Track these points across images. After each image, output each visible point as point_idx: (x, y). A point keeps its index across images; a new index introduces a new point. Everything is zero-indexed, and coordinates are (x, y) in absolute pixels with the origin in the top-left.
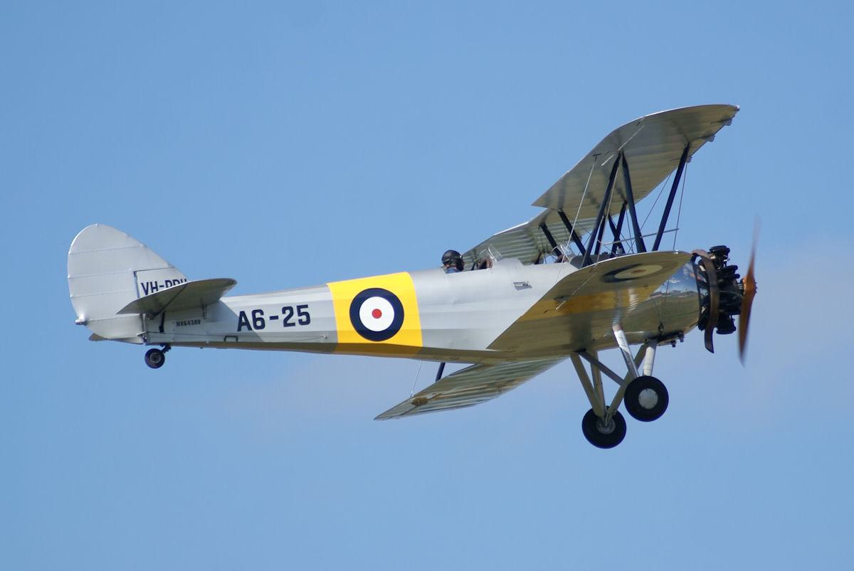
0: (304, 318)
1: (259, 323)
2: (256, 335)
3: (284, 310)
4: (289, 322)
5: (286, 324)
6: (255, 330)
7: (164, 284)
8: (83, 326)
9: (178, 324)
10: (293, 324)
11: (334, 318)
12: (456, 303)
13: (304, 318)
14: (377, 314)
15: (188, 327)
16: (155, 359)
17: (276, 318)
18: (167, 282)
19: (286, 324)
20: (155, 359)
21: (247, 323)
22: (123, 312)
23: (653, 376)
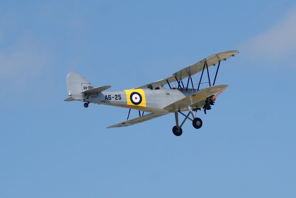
0: (120, 98)
1: (110, 98)
2: (109, 101)
3: (115, 95)
4: (116, 99)
5: (116, 99)
9: (92, 97)
10: (117, 99)
11: (126, 99)
12: (153, 97)
13: (120, 98)
14: (136, 98)
16: (86, 105)
17: (114, 97)
18: (89, 87)
19: (116, 99)
20: (86, 105)
21: (107, 98)
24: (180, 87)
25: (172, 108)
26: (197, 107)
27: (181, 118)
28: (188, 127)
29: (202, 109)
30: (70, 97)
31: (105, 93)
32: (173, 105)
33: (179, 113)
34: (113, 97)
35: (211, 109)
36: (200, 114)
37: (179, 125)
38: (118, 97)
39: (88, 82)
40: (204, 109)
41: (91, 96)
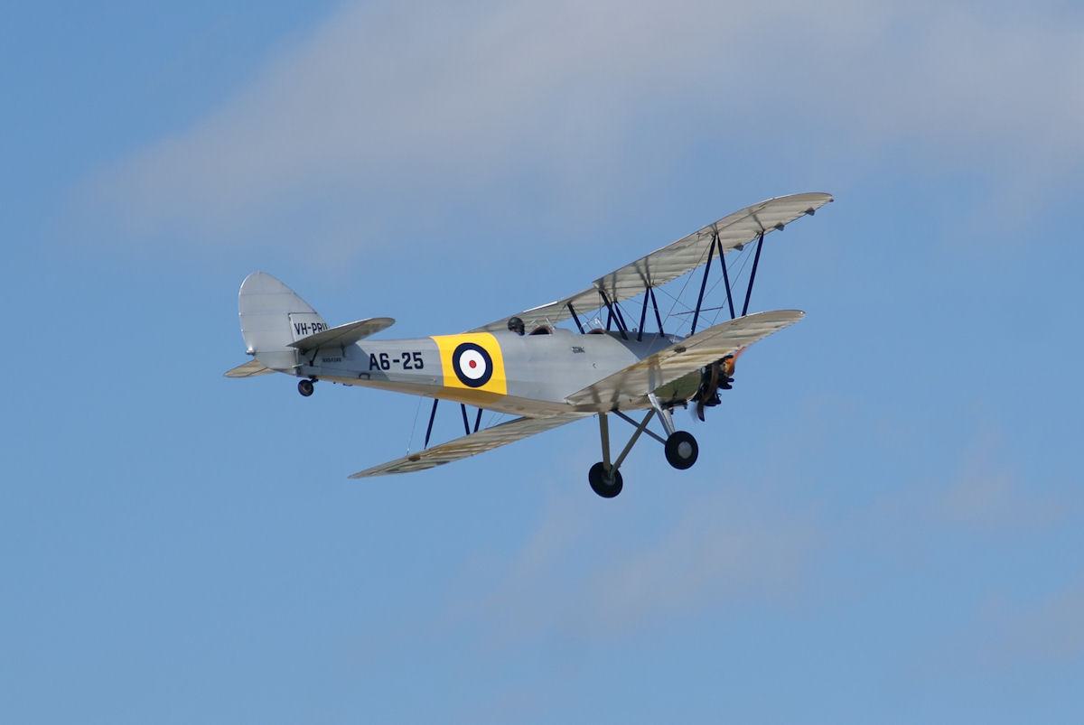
0: (418, 363)
1: (385, 365)
2: (384, 375)
3: (404, 355)
4: (407, 365)
5: (405, 368)
7: (310, 326)
8: (251, 356)
9: (324, 360)
10: (411, 368)
13: (418, 363)
14: (473, 364)
15: (332, 363)
16: (307, 388)
17: (398, 361)
19: (405, 368)
20: (306, 388)
21: (376, 364)
22: (289, 346)
23: (676, 431)
24: (614, 328)
25: (589, 401)
26: (675, 394)
27: (620, 432)
28: (645, 465)
29: (691, 404)
30: (251, 357)
31: (369, 345)
32: (594, 390)
33: (611, 416)
34: (395, 361)
35: (719, 402)
36: (683, 419)
37: (613, 461)
39: (309, 306)
40: (697, 402)
41: (322, 355)
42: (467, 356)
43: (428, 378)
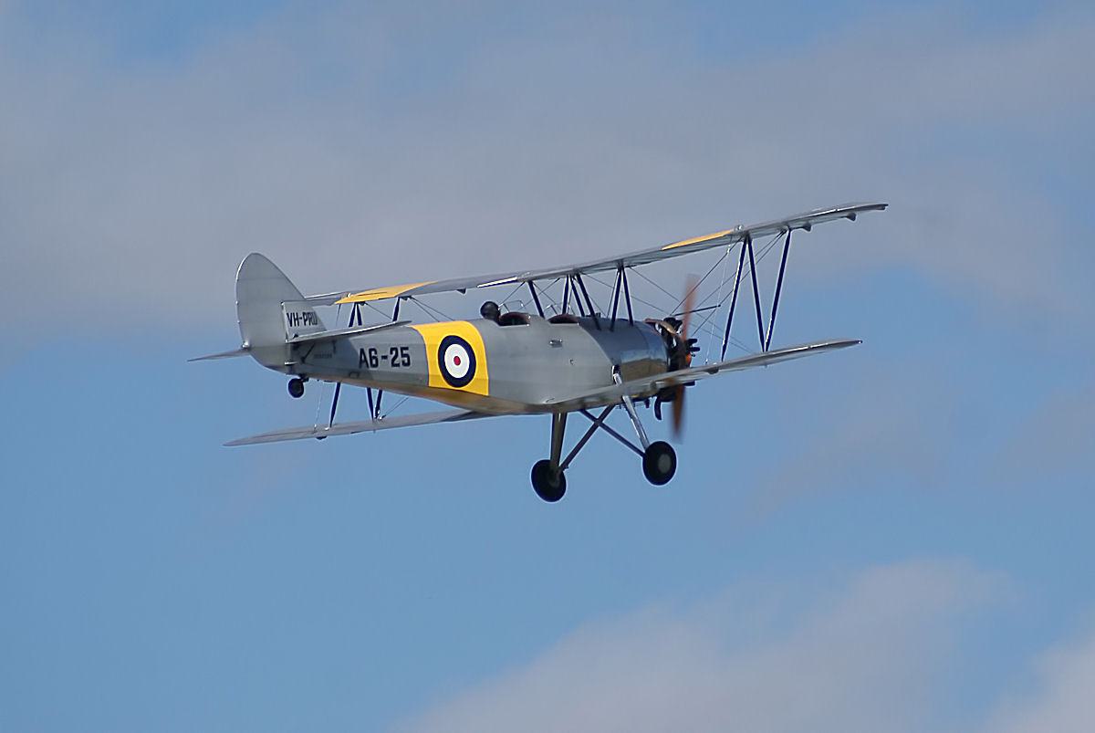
0: (406, 361)
1: (374, 362)
2: (369, 373)
3: (392, 350)
4: (396, 362)
5: (393, 365)
6: (371, 369)
7: (302, 316)
9: (316, 356)
10: (398, 365)
13: (406, 359)
14: (457, 361)
18: (304, 314)
19: (393, 365)
20: (296, 388)
27: (577, 424)
38: (402, 354)
42: (455, 350)
43: (415, 377)
